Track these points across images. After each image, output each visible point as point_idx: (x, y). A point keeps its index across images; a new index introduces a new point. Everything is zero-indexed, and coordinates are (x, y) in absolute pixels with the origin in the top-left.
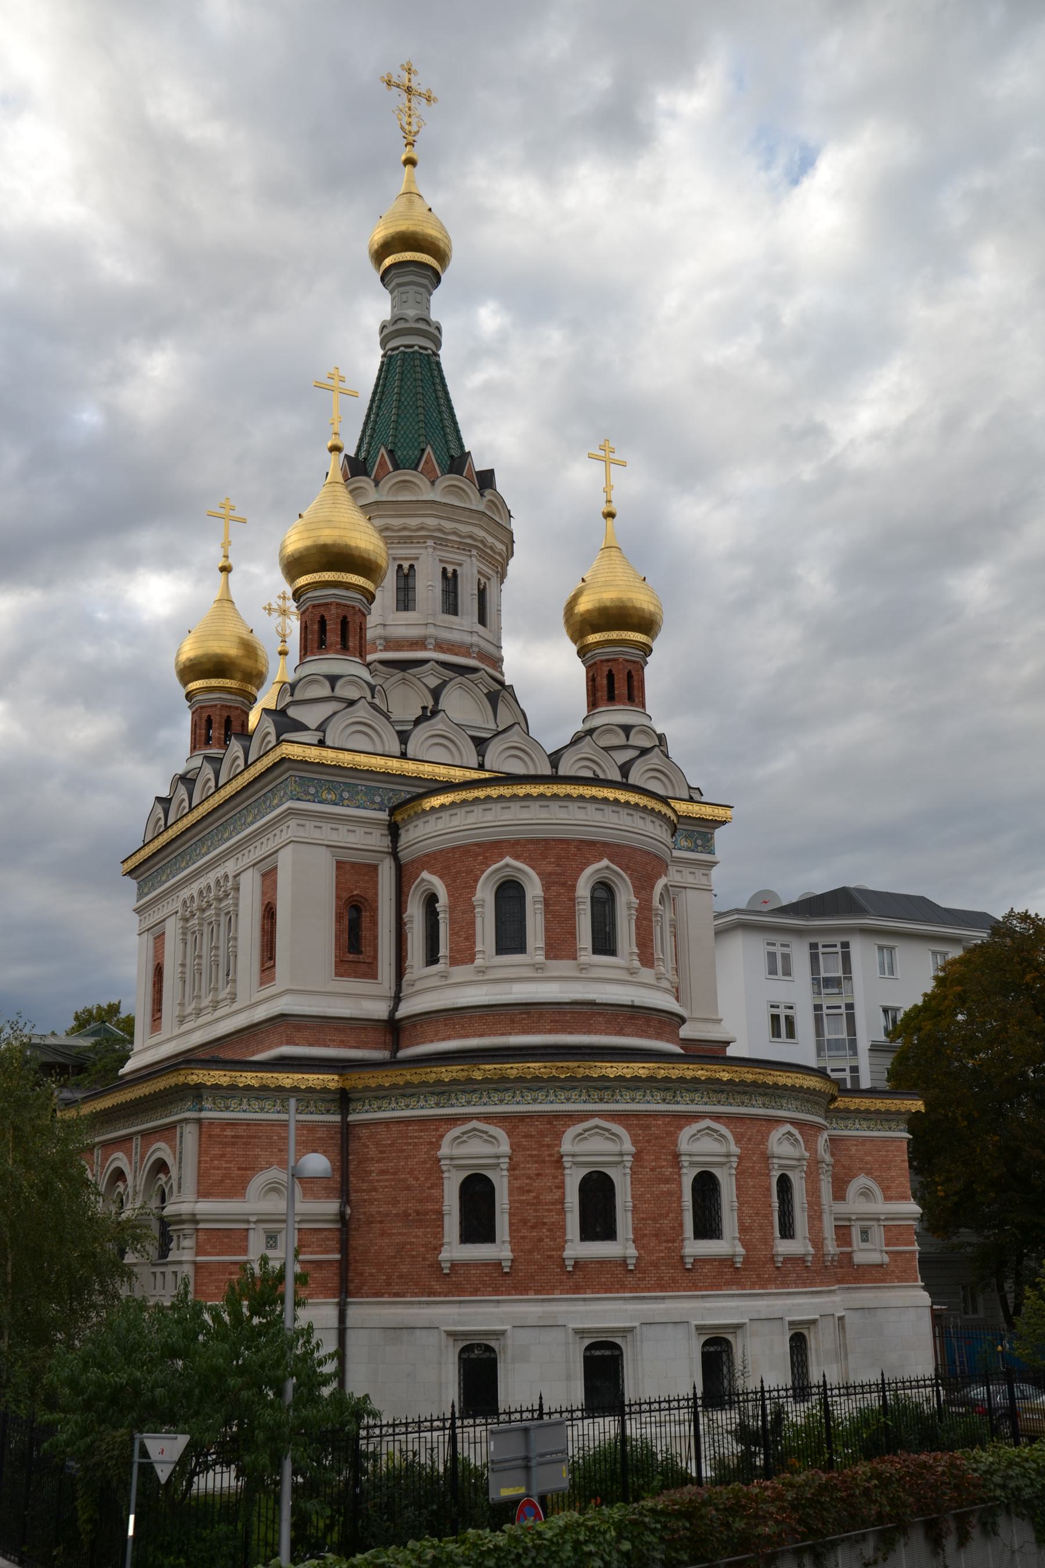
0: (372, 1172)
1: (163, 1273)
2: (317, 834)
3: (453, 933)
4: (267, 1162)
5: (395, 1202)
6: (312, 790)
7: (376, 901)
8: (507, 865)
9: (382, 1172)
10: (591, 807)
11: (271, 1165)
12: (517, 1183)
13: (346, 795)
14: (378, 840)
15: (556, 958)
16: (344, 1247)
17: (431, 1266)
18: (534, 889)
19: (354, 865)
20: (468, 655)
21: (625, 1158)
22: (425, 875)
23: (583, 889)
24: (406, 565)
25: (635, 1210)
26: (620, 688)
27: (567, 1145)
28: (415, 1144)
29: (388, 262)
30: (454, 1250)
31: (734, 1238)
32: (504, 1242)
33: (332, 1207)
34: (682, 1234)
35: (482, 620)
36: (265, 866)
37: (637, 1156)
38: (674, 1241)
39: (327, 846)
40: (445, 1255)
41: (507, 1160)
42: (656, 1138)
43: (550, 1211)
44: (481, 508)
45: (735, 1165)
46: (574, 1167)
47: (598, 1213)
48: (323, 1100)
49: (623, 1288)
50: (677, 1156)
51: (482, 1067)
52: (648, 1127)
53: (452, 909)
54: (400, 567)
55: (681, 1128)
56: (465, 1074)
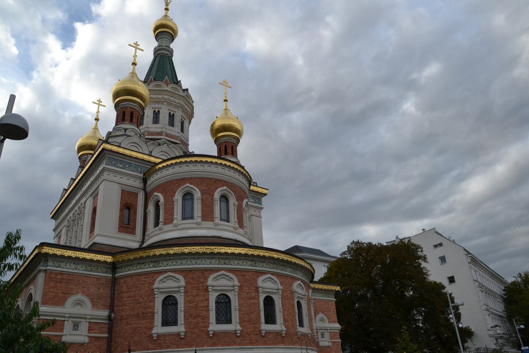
0: (124, 297)
2: (114, 178)
3: (165, 213)
4: (76, 292)
6: (114, 163)
7: (136, 206)
8: (187, 186)
9: (128, 297)
10: (220, 167)
11: (78, 293)
12: (188, 299)
13: (127, 166)
14: (138, 184)
15: (206, 220)
16: (110, 331)
17: (148, 337)
18: (197, 194)
19: (128, 192)
20: (177, 139)
21: (236, 288)
22: (155, 193)
23: (217, 195)
24: (157, 110)
25: (240, 310)
26: (229, 150)
27: (210, 282)
28: (143, 284)
29: (157, 32)
30: (159, 329)
31: (281, 324)
32: (181, 324)
33: (106, 313)
34: (260, 321)
35: (182, 130)
37: (240, 287)
38: (256, 324)
39: (118, 183)
40: (154, 331)
41: (183, 288)
42: (248, 281)
43: (201, 310)
44: (183, 95)
45: (281, 293)
46: (213, 292)
47: (224, 313)
48: (104, 267)
49: (235, 344)
50: (257, 288)
51: (173, 248)
52: (245, 276)
53: (165, 205)
54: (155, 111)
55: (259, 277)
56: (166, 251)
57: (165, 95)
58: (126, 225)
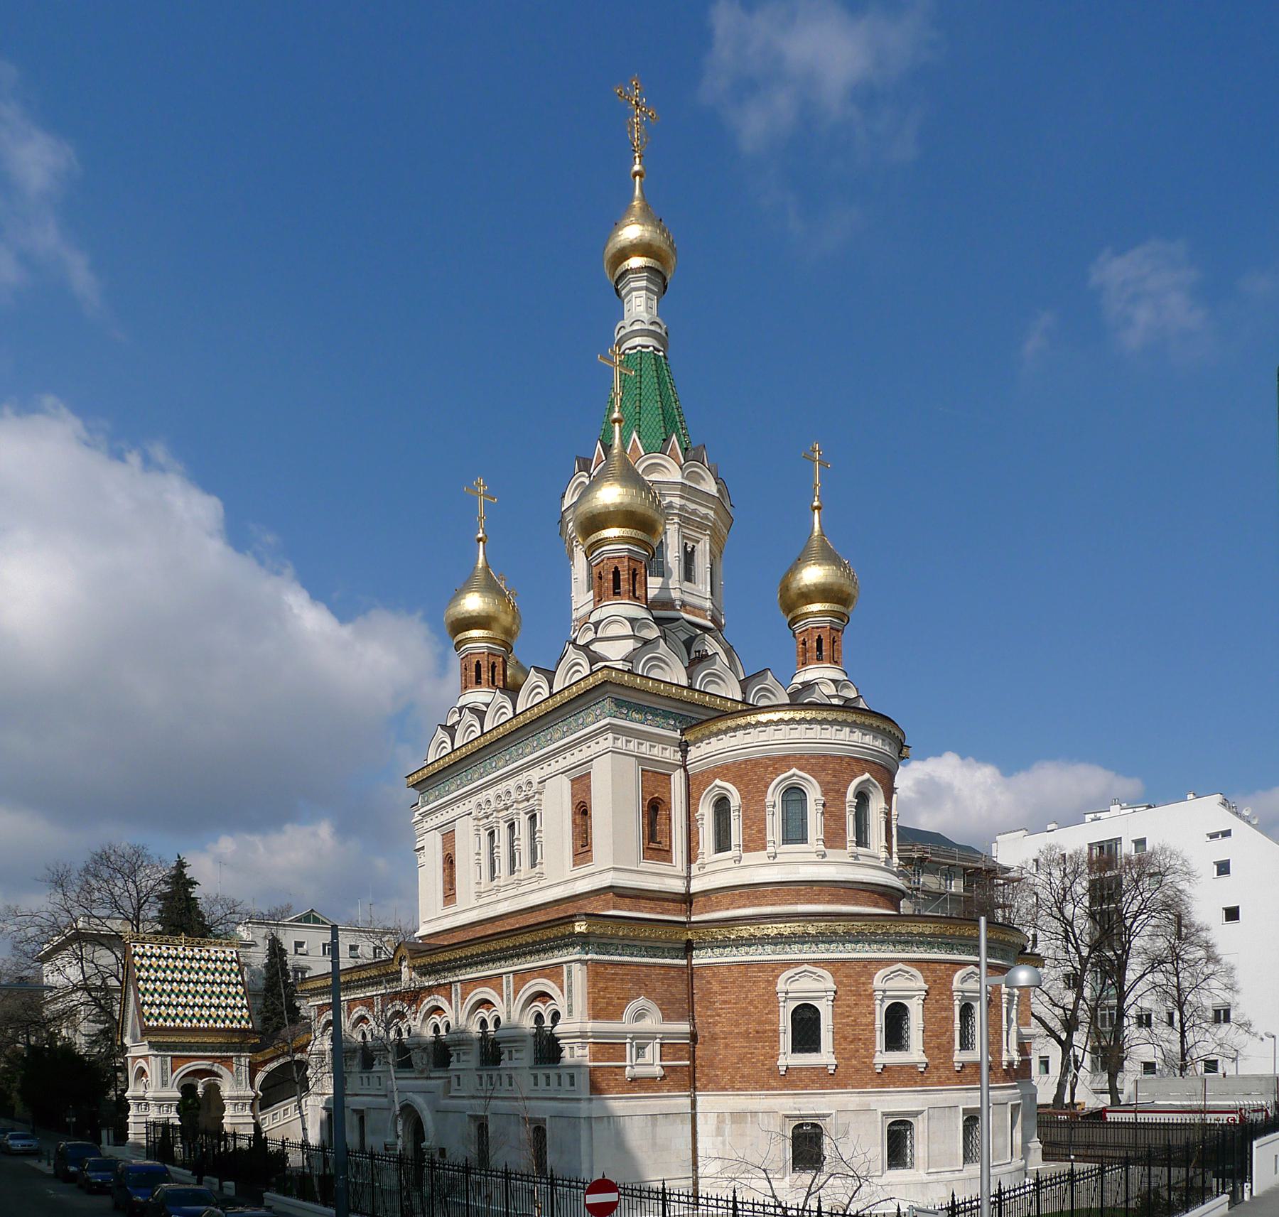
1: (548, 1077)
5: (737, 1025)
12: (839, 1011)
14: (671, 755)
15: (831, 847)
18: (814, 794)
22: (718, 782)
27: (877, 982)
36: (576, 773)
49: (916, 1084)
55: (955, 971)
57: (673, 495)
58: (655, 843)
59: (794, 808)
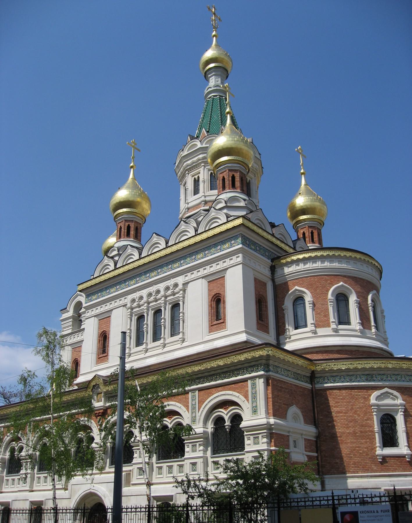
6: (248, 242)
13: (258, 248)
19: (260, 281)
59: (342, 304)
